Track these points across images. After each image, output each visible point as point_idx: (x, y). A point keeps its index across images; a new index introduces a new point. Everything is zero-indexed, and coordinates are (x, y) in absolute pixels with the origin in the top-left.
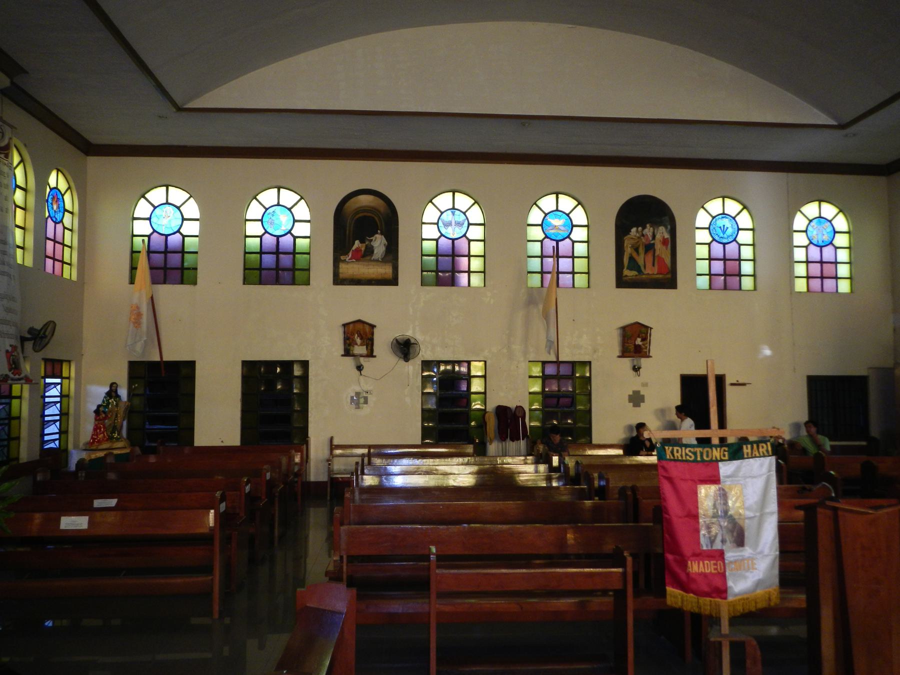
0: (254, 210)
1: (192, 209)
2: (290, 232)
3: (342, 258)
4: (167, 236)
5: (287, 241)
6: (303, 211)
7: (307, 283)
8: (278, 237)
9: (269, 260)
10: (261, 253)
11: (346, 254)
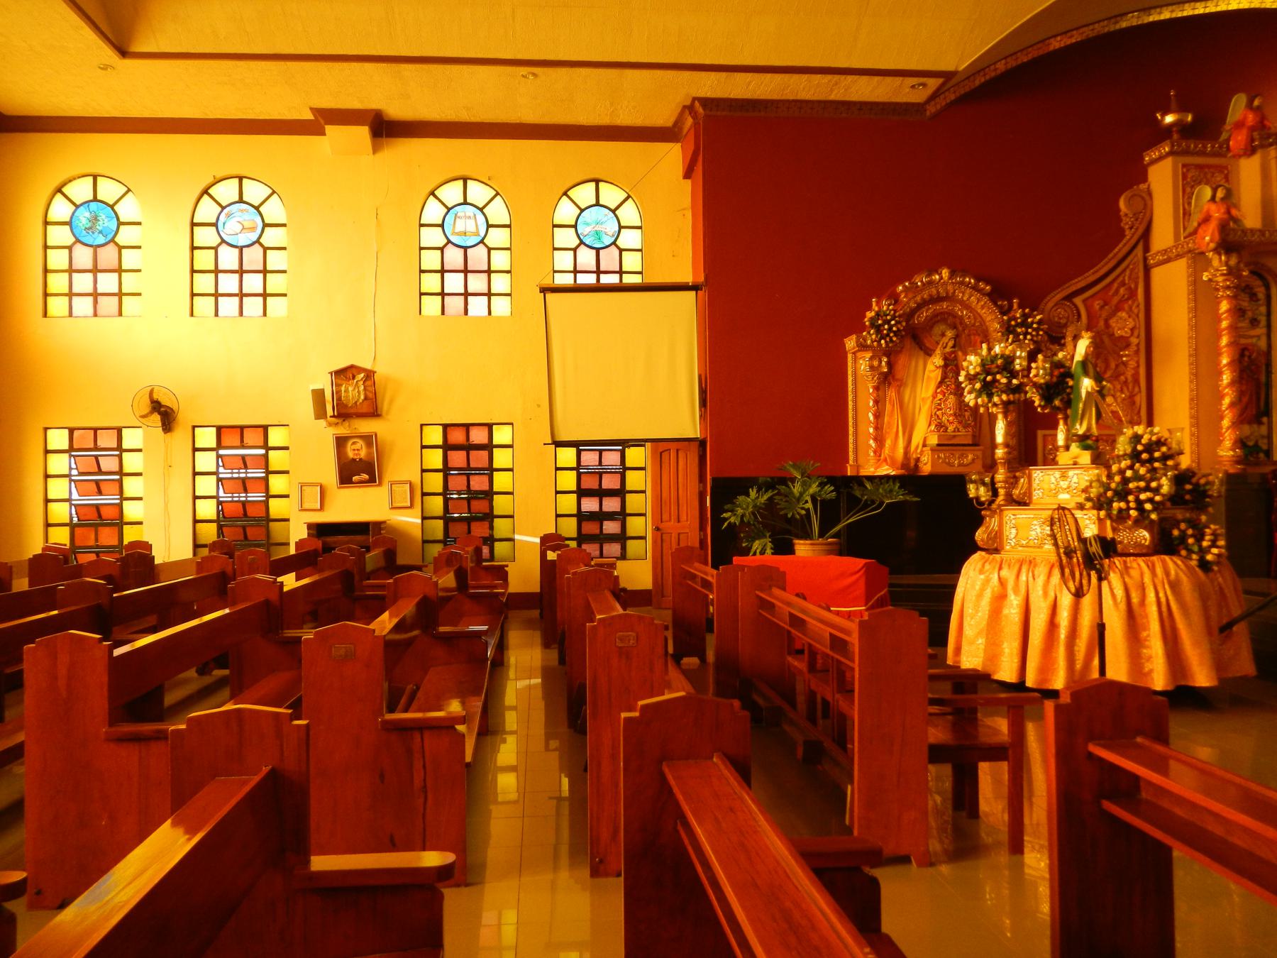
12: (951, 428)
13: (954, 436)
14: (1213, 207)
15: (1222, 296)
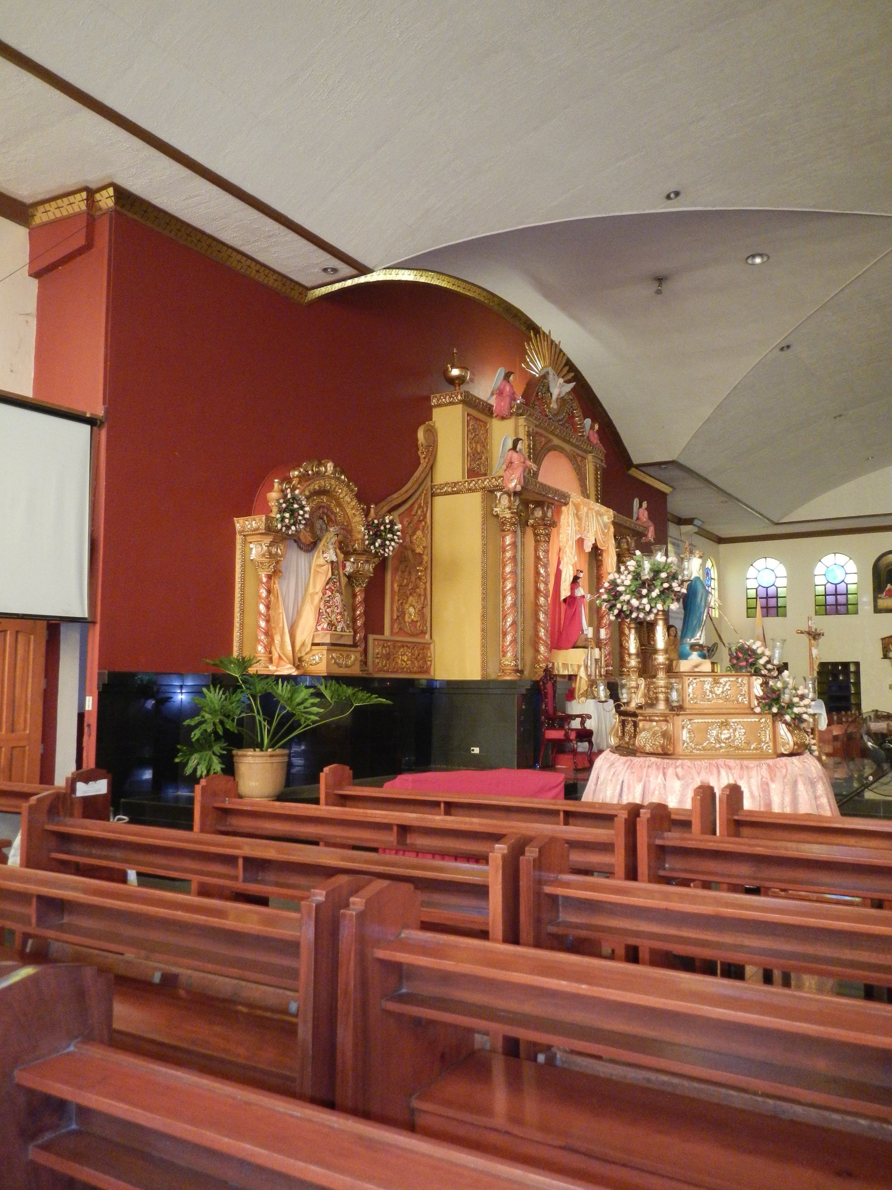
0: (819, 569)
1: (781, 570)
2: (843, 581)
3: (879, 596)
4: (767, 588)
5: (841, 588)
6: (852, 567)
7: (856, 613)
8: (836, 585)
9: (831, 600)
10: (826, 595)
11: (882, 593)
12: (339, 628)
13: (342, 636)
14: (515, 455)
15: (509, 530)
